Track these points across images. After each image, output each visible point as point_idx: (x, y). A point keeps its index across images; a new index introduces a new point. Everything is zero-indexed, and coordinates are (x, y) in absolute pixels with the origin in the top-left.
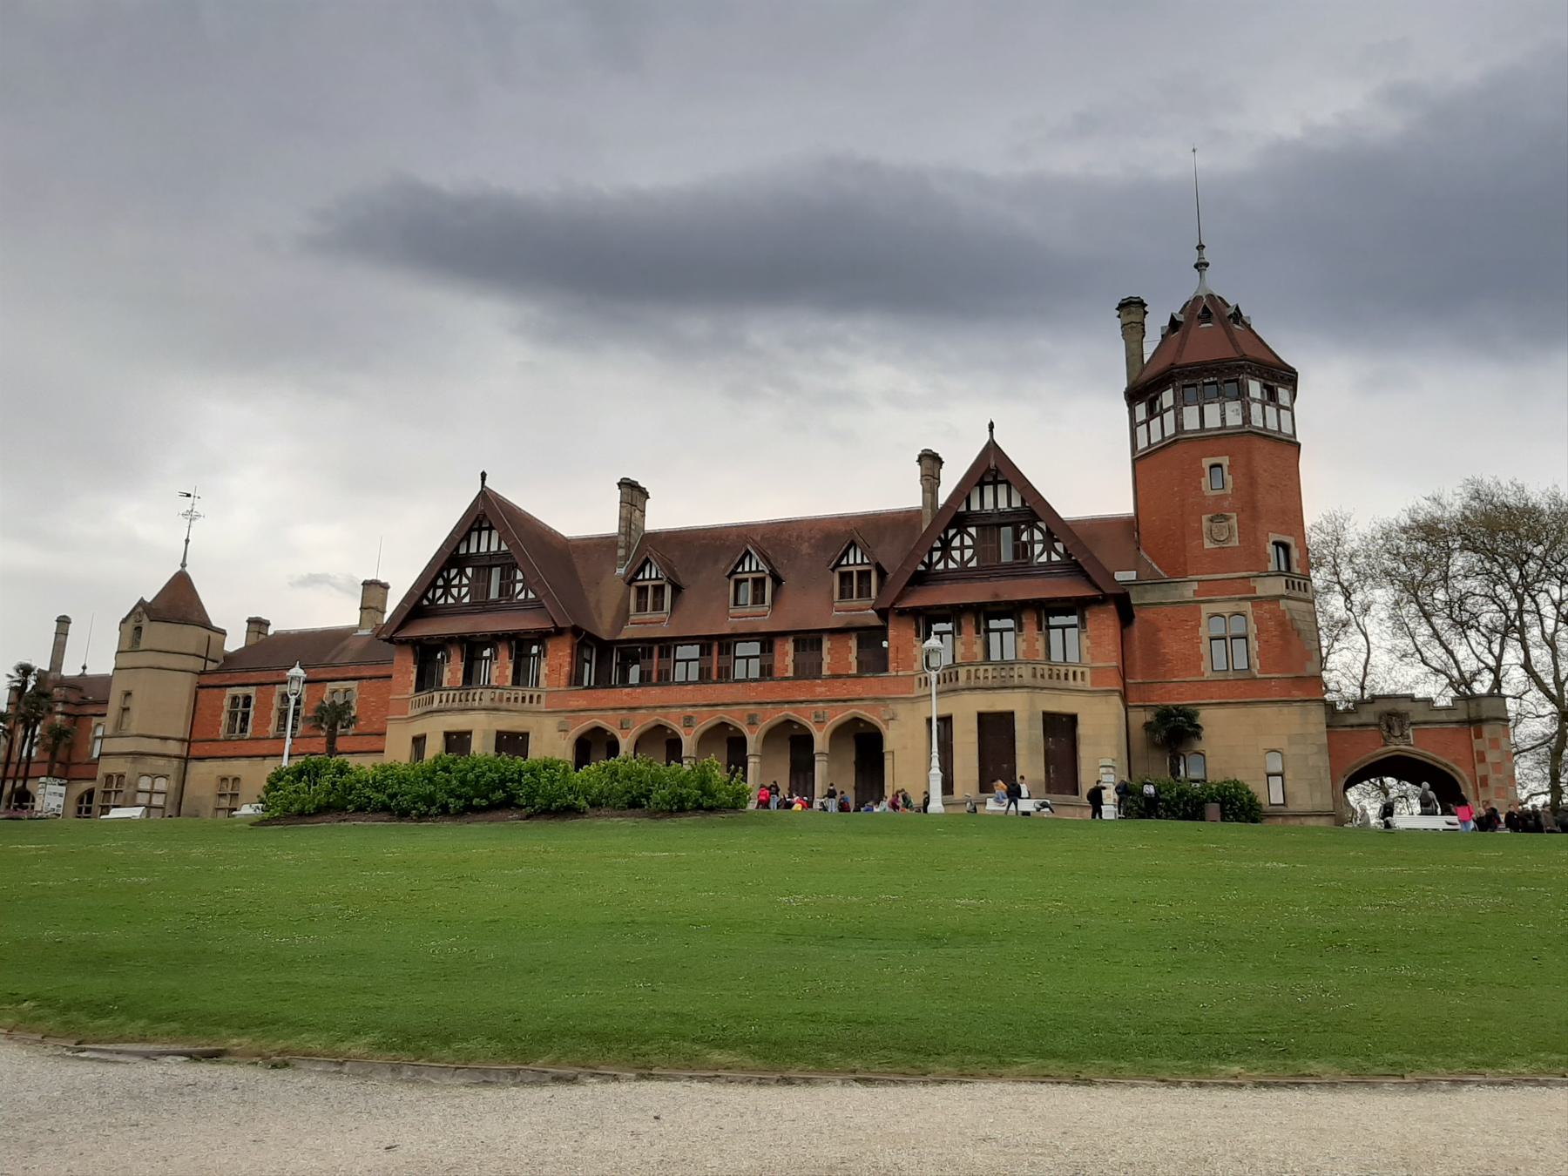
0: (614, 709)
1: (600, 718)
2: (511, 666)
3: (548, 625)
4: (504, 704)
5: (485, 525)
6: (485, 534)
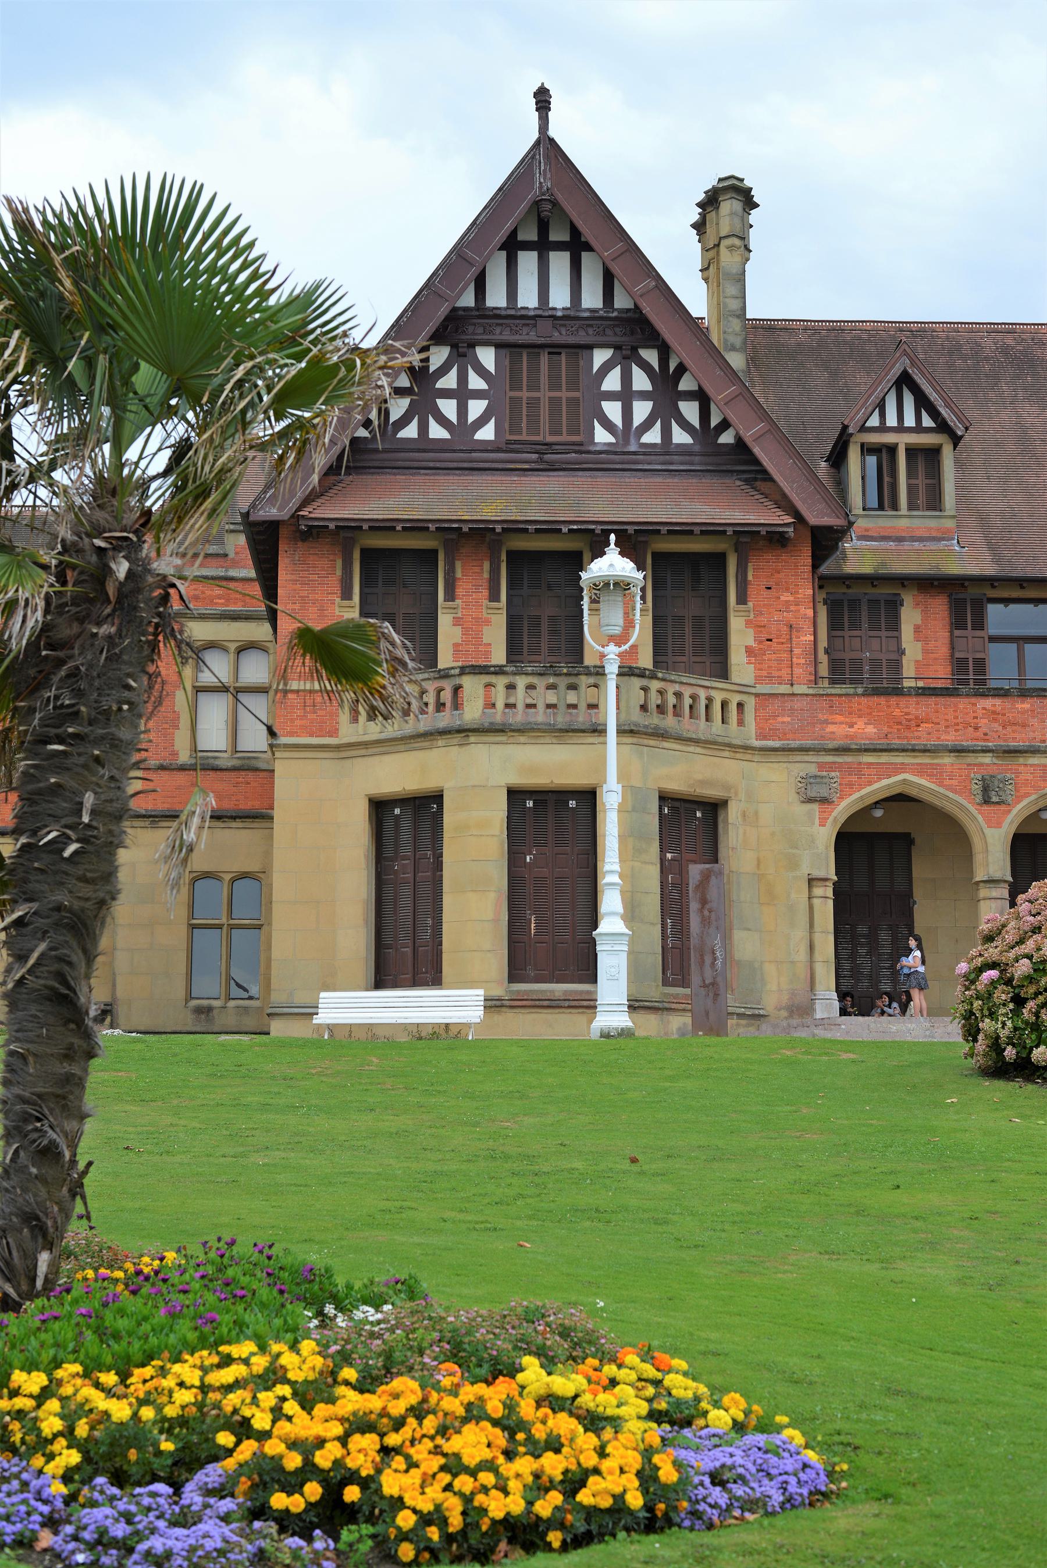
0: (958, 751)
1: (920, 770)
2: (500, 620)
3: (779, 518)
4: (669, 722)
6: (527, 261)
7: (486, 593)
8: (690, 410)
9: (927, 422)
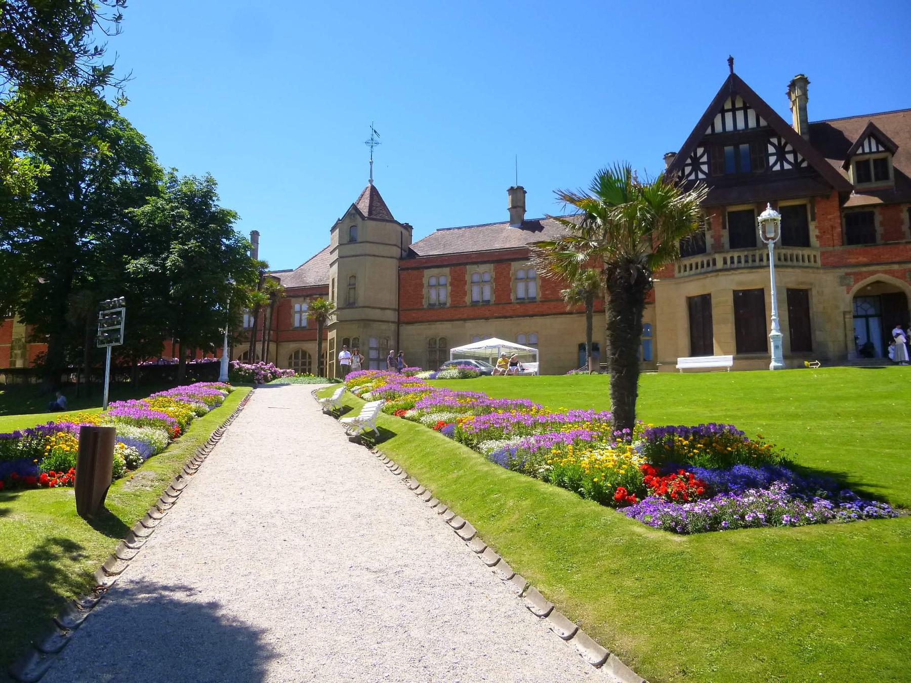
1: (886, 272)
5: (728, 106)
6: (729, 116)
7: (721, 226)
8: (790, 157)
9: (881, 149)
